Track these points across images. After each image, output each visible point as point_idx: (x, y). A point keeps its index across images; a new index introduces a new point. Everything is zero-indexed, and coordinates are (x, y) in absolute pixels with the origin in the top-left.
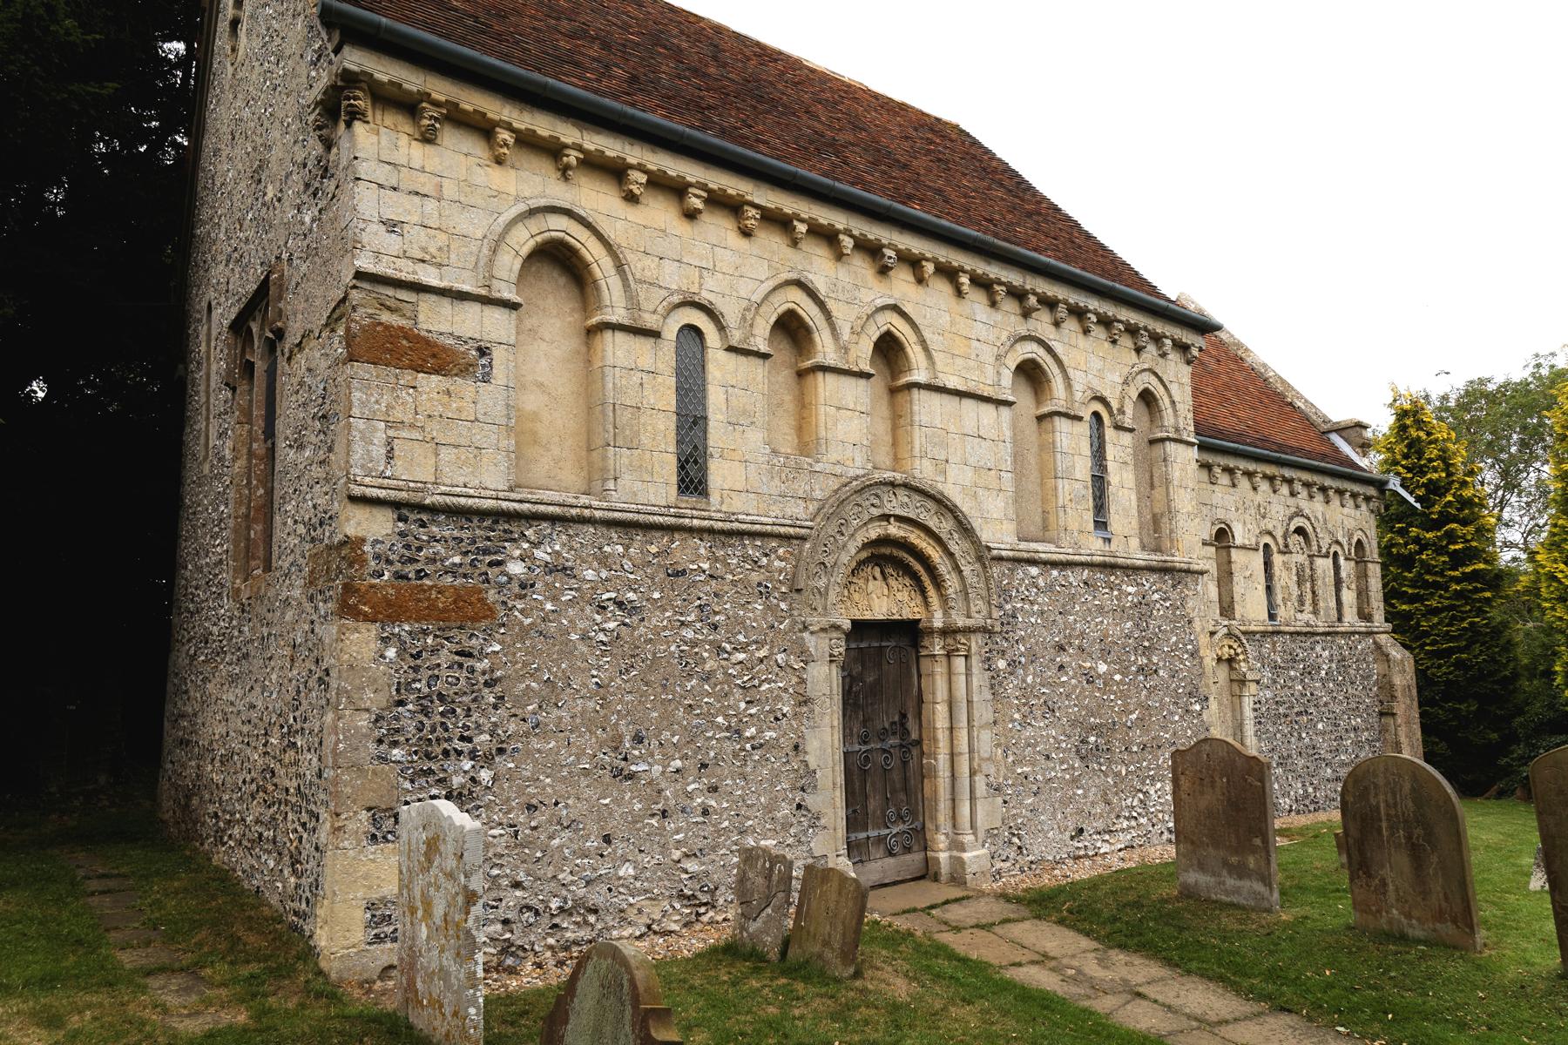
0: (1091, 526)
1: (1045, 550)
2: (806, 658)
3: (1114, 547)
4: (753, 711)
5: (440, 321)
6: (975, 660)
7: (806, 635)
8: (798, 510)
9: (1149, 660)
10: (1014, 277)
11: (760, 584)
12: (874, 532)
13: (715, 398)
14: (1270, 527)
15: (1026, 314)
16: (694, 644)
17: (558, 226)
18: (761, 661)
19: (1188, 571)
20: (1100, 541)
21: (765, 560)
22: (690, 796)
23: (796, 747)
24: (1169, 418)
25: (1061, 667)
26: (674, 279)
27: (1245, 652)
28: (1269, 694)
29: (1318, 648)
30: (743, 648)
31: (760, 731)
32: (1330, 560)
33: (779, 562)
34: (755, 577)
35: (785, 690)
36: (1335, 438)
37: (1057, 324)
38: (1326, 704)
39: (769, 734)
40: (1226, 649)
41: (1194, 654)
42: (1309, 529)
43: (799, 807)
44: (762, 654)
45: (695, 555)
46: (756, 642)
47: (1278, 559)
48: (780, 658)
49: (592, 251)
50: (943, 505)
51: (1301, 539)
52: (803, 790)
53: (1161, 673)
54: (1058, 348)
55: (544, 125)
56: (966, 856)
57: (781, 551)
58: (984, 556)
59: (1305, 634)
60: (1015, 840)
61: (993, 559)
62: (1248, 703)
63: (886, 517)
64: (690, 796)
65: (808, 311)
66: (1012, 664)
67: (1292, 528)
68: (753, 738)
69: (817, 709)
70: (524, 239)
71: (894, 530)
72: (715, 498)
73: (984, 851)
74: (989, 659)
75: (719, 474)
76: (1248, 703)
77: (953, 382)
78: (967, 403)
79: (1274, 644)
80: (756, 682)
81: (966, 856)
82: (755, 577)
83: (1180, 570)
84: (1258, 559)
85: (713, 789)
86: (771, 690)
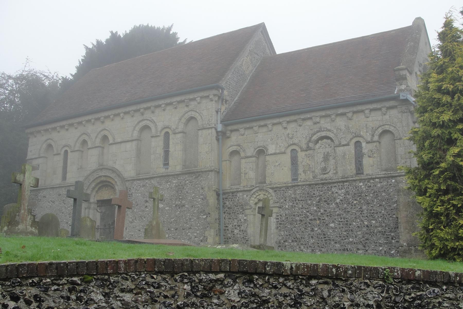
0: (162, 166)
3: (169, 170)
5: (35, 163)
9: (181, 202)
10: (134, 108)
12: (98, 181)
13: (69, 161)
14: (296, 141)
15: (143, 114)
19: (202, 172)
20: (164, 169)
24: (200, 123)
25: (146, 207)
27: (272, 196)
32: (352, 148)
37: (153, 112)
38: (338, 215)
40: (262, 195)
41: (204, 199)
42: (331, 135)
47: (301, 155)
49: (53, 144)
50: (113, 170)
51: (329, 141)
53: (187, 206)
54: (154, 118)
58: (124, 180)
59: (323, 184)
61: (126, 181)
63: (101, 176)
67: (315, 137)
70: (45, 146)
71: (103, 179)
72: (67, 180)
75: (69, 175)
77: (119, 140)
78: (123, 144)
79: (295, 191)
83: (197, 172)
84: (287, 159)
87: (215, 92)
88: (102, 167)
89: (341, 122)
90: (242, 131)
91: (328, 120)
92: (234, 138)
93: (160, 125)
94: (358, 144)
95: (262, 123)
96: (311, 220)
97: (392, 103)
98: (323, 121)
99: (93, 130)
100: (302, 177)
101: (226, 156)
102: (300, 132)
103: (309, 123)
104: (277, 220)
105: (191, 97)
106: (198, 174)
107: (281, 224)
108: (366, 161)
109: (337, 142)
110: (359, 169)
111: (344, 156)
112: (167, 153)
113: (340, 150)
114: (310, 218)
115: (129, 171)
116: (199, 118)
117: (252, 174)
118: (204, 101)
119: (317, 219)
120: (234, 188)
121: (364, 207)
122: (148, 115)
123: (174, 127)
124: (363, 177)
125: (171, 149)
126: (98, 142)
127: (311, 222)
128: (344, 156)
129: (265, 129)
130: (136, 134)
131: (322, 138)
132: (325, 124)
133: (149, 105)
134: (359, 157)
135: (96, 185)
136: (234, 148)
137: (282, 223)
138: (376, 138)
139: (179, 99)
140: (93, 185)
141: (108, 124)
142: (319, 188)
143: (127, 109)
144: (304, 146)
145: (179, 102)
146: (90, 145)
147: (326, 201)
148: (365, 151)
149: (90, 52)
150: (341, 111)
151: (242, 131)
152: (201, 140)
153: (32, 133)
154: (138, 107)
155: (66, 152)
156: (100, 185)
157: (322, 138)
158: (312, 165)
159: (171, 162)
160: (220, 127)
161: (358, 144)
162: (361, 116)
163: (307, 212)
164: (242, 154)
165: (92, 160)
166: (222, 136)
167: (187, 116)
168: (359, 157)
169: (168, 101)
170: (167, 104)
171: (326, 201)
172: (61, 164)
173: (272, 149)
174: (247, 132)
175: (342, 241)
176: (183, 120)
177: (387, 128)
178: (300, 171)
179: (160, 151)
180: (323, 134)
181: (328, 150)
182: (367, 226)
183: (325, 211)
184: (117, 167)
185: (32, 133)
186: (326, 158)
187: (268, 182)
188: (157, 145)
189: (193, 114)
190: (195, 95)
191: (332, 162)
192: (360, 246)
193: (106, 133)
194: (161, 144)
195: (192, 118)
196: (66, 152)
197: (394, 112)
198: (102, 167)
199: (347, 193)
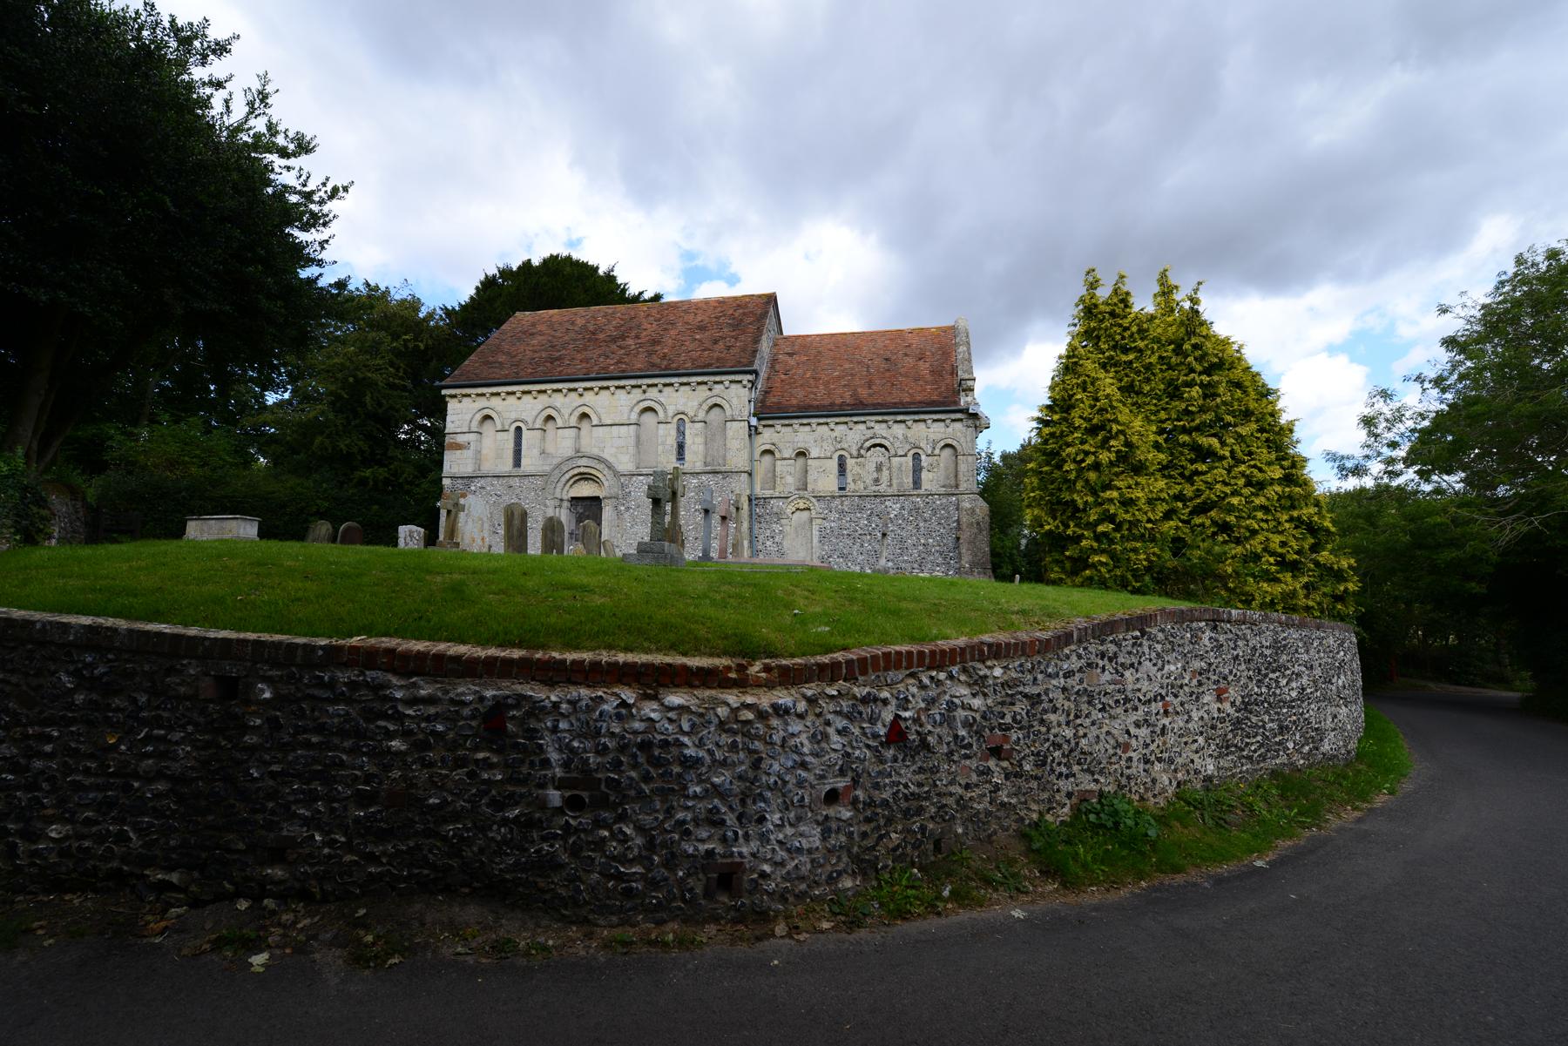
1: (645, 471)
5: (461, 439)
8: (548, 468)
10: (633, 382)
12: (576, 471)
17: (486, 412)
24: (729, 412)
26: (514, 416)
33: (540, 482)
42: (887, 443)
45: (516, 482)
47: (850, 462)
49: (493, 415)
50: (600, 460)
55: (480, 390)
58: (617, 474)
62: (815, 528)
65: (554, 413)
66: (628, 509)
67: (868, 444)
70: (479, 417)
71: (582, 470)
76: (815, 528)
84: (834, 463)
87: (750, 377)
88: (579, 454)
89: (899, 430)
90: (778, 428)
91: (884, 425)
92: (767, 437)
93: (671, 410)
94: (916, 457)
95: (805, 421)
97: (959, 416)
98: (877, 426)
99: (565, 402)
100: (851, 486)
101: (757, 456)
102: (852, 434)
103: (862, 427)
105: (718, 378)
106: (726, 474)
108: (924, 475)
109: (892, 452)
110: (917, 483)
111: (900, 469)
112: (681, 447)
113: (895, 460)
115: (625, 464)
116: (726, 406)
117: (790, 479)
118: (734, 386)
120: (768, 493)
122: (652, 393)
123: (691, 414)
124: (922, 492)
125: (688, 440)
126: (573, 421)
128: (900, 469)
129: (807, 428)
130: (634, 417)
131: (875, 446)
132: (880, 429)
133: (655, 381)
134: (917, 470)
136: (767, 447)
138: (937, 451)
139: (700, 379)
140: (567, 476)
141: (589, 396)
143: (622, 383)
144: (855, 453)
145: (699, 383)
146: (560, 423)
148: (924, 464)
149: (488, 284)
150: (900, 418)
151: (778, 428)
152: (730, 433)
153: (454, 396)
154: (639, 382)
155: (519, 429)
157: (875, 446)
158: (862, 473)
159: (688, 456)
160: (754, 421)
161: (916, 457)
162: (922, 425)
164: (777, 455)
165: (562, 443)
166: (753, 432)
167: (711, 402)
168: (917, 470)
169: (685, 380)
170: (682, 384)
172: (511, 445)
173: (814, 453)
174: (785, 429)
176: (705, 407)
177: (949, 441)
178: (850, 480)
179: (672, 441)
180: (878, 441)
181: (881, 459)
184: (606, 456)
185: (454, 396)
186: (879, 468)
187: (810, 487)
188: (668, 435)
189: (718, 400)
190: (723, 378)
191: (885, 473)
193: (587, 410)
194: (674, 433)
195: (716, 405)
196: (519, 429)
197: (958, 425)
198: (579, 454)
199: (903, 508)
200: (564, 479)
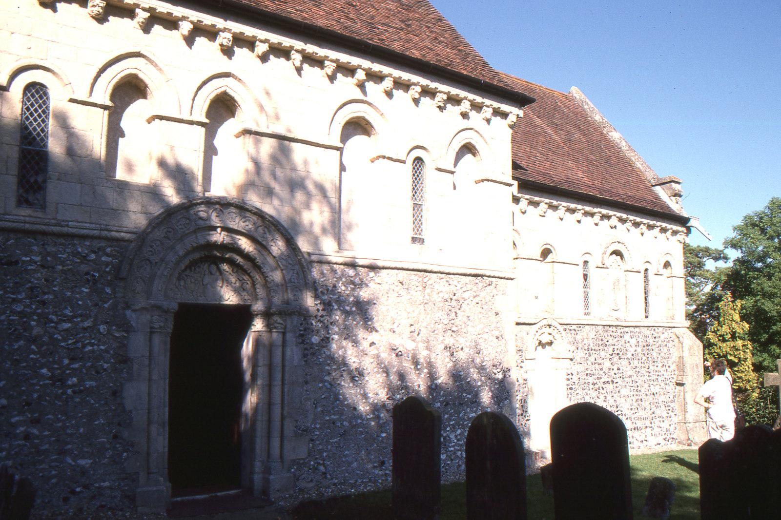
2: (127, 327)
4: (76, 366)
6: (289, 336)
7: (128, 313)
11: (87, 274)
16: (22, 314)
18: (85, 329)
21: (93, 256)
22: (15, 426)
23: (114, 393)
28: (581, 368)
29: (627, 337)
30: (69, 320)
31: (81, 380)
34: (84, 268)
35: (107, 351)
36: (658, 190)
38: (630, 376)
39: (88, 384)
43: (115, 437)
44: (86, 324)
46: (81, 315)
48: (103, 328)
52: (119, 424)
56: (272, 477)
57: (109, 250)
60: (322, 468)
64: (15, 426)
68: (74, 385)
69: (135, 367)
73: (288, 475)
74: (302, 335)
80: (80, 345)
81: (272, 477)
82: (84, 268)
85: (35, 422)
86: (93, 351)
96: (604, 383)
104: (568, 382)
107: (571, 389)
114: (603, 380)
119: (611, 382)
121: (651, 367)
127: (604, 386)
135: (188, 253)
137: (573, 387)
140: (181, 250)
142: (613, 332)
147: (618, 354)
156: (197, 256)
163: (602, 369)
171: (618, 354)
175: (633, 416)
182: (653, 394)
183: (619, 369)
192: (648, 423)
200: (172, 257)
